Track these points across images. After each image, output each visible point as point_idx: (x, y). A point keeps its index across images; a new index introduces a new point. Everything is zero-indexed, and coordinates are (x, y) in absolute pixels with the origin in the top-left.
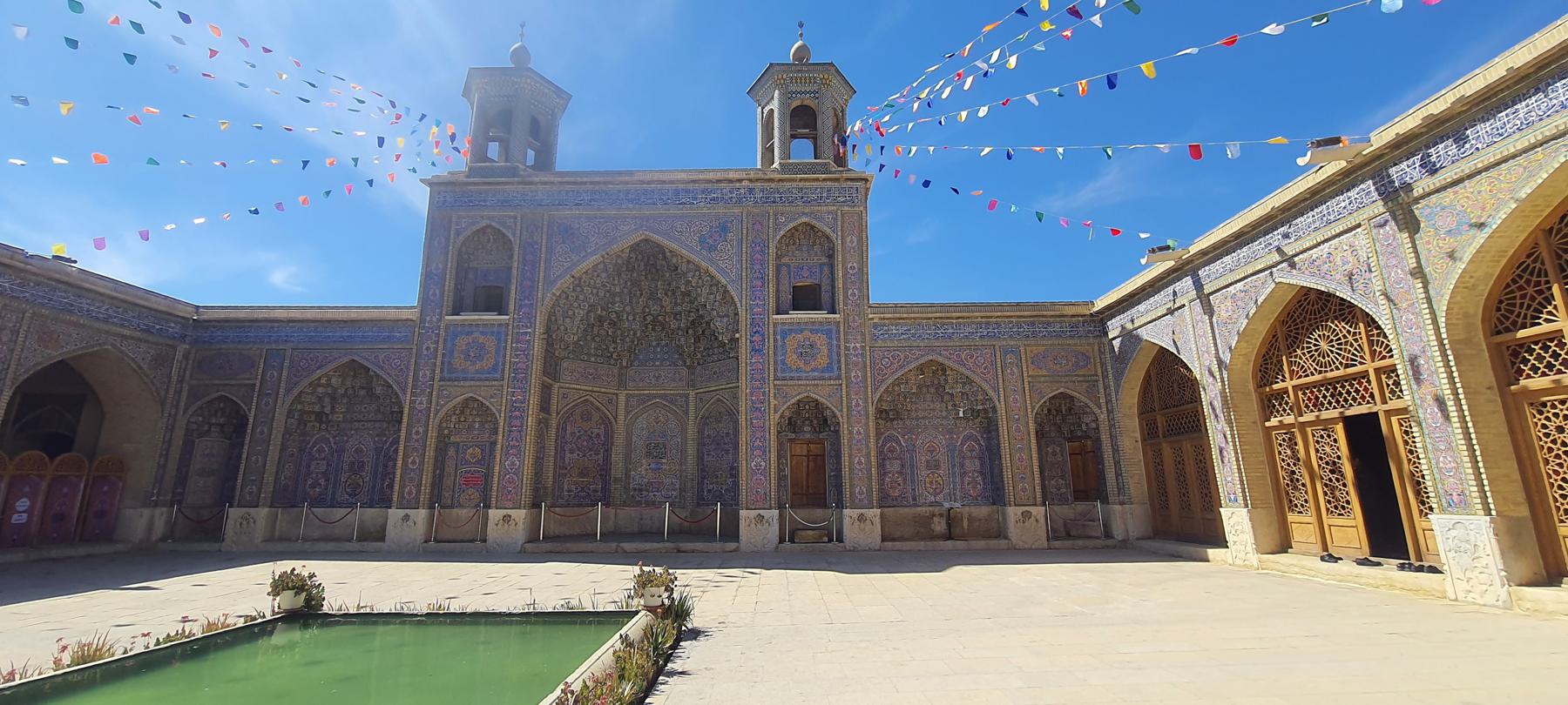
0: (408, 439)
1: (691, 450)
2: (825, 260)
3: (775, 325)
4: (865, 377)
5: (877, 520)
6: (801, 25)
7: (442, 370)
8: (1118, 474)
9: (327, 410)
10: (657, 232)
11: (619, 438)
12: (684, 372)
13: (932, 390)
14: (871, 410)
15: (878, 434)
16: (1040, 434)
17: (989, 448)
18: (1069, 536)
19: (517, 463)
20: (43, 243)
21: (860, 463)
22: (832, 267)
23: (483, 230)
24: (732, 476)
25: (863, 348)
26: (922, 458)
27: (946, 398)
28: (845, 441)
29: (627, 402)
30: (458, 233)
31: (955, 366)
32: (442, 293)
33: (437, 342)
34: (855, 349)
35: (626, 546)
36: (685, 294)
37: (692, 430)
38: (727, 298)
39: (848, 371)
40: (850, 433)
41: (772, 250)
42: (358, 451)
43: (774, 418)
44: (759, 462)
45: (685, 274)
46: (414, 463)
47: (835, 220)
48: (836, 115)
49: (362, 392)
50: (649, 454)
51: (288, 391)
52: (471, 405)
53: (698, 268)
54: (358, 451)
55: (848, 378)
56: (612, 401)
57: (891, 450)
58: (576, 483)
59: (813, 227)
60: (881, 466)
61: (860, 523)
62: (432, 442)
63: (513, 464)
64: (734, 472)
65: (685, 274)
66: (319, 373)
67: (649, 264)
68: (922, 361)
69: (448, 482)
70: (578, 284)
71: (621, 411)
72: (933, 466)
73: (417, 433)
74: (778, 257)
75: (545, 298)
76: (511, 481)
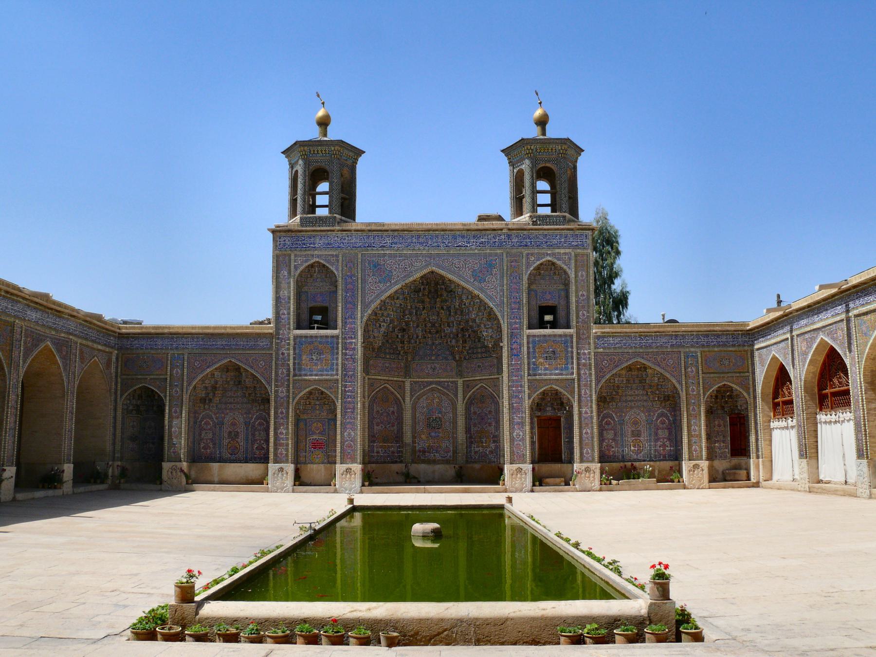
0: (275, 418)
1: (461, 422)
2: (562, 287)
3: (528, 336)
4: (590, 374)
7: (294, 369)
8: (757, 440)
9: (211, 396)
10: (439, 267)
11: (407, 416)
12: (454, 364)
13: (637, 381)
14: (594, 397)
16: (710, 412)
17: (675, 422)
18: (725, 480)
20: (30, 281)
21: (586, 433)
23: (312, 266)
24: (494, 442)
26: (628, 429)
30: (296, 268)
33: (288, 349)
34: (584, 354)
38: (491, 316)
39: (578, 369)
40: (580, 413)
42: (234, 424)
43: (527, 403)
44: (516, 433)
45: (460, 297)
47: (570, 259)
50: (429, 425)
51: (189, 384)
53: (471, 293)
54: (234, 424)
56: (401, 387)
57: (608, 423)
58: (381, 447)
59: (553, 264)
60: (601, 434)
63: (349, 434)
66: (209, 370)
69: (302, 445)
71: (408, 394)
72: (637, 434)
73: (282, 413)
76: (350, 446)
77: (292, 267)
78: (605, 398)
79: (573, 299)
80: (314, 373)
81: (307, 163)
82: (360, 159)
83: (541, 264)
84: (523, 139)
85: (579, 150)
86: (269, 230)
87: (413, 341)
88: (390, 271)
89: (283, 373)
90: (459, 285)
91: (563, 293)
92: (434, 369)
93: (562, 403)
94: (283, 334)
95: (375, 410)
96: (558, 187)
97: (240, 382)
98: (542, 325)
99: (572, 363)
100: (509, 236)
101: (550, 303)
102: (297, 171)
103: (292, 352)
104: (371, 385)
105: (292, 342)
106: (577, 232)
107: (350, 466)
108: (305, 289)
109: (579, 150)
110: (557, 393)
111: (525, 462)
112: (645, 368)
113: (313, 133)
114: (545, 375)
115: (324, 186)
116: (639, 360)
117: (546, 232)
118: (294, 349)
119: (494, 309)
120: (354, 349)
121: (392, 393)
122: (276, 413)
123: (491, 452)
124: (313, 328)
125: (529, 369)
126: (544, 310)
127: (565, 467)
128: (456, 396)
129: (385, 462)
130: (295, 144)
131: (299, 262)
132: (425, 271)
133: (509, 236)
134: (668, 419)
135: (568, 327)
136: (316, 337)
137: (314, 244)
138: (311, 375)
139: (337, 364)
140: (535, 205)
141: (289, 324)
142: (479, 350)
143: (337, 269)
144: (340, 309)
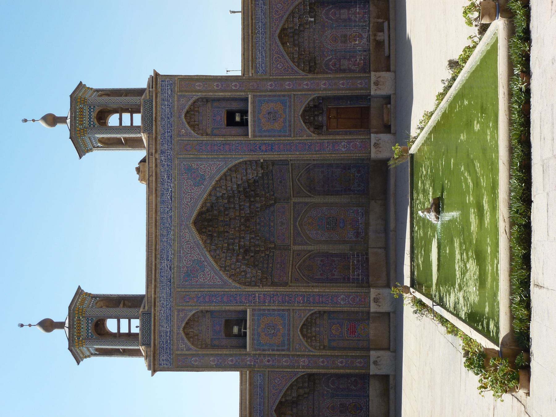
0: (327, 368)
2: (209, 104)
4: (290, 80)
5: (378, 74)
6: (25, 121)
7: (283, 350)
11: (324, 248)
12: (278, 205)
13: (296, 37)
14: (310, 76)
15: (324, 72)
19: (341, 297)
21: (343, 84)
22: (214, 100)
23: (187, 334)
24: (349, 169)
25: (270, 80)
27: (302, 28)
28: (329, 93)
29: (299, 244)
30: (189, 349)
31: (283, 22)
32: (231, 355)
33: (265, 355)
34: (271, 85)
35: (392, 226)
36: (229, 202)
37: (318, 199)
38: (235, 169)
39: (284, 91)
41: (205, 138)
43: (315, 137)
45: (218, 198)
46: (342, 362)
48: (101, 96)
49: (295, 410)
52: (305, 333)
53: (214, 188)
55: (290, 90)
57: (334, 65)
58: (353, 272)
60: (344, 71)
61: (380, 85)
62: (329, 353)
63: (343, 299)
64: (346, 167)
65: (218, 198)
67: (207, 222)
68: (280, 44)
70: (224, 268)
71: (305, 247)
73: (323, 362)
74: (207, 135)
75: (234, 287)
77: (187, 352)
78: (310, 67)
79: (221, 94)
80: (286, 332)
81: (88, 339)
82: (86, 290)
83: (188, 123)
84: (70, 138)
85: (81, 85)
86: (153, 375)
87: (257, 243)
88: (194, 261)
89: (286, 361)
90: (206, 199)
91: (216, 104)
92: (283, 224)
93: (315, 106)
94: (250, 361)
95: (320, 277)
96: (115, 106)
97: (293, 402)
98: (244, 123)
99: (279, 96)
100: (162, 152)
101: (224, 116)
102: (97, 350)
103: (267, 352)
104: (297, 280)
105: (258, 352)
106: (159, 90)
107: (372, 299)
108: (208, 341)
109: (81, 85)
110: (305, 111)
111: (370, 138)
112: (283, 30)
113: (61, 336)
114: (290, 121)
115: (111, 325)
116: (277, 35)
117: (159, 118)
118: (264, 350)
119: (230, 166)
120: (264, 295)
121: (304, 261)
122: (323, 367)
123: (359, 172)
124: (245, 333)
125: (284, 136)
126: (231, 121)
127: (374, 104)
128: (306, 204)
129: (367, 269)
130: (71, 351)
131: (183, 346)
132: (194, 229)
133: (162, 152)
134: (331, 9)
135: (246, 100)
136: (253, 330)
137: (167, 332)
138: (289, 335)
139: (279, 310)
140: (132, 128)
141: (240, 355)
142: (266, 182)
143: (191, 311)
144: (227, 308)
